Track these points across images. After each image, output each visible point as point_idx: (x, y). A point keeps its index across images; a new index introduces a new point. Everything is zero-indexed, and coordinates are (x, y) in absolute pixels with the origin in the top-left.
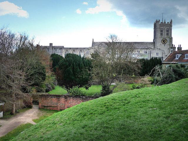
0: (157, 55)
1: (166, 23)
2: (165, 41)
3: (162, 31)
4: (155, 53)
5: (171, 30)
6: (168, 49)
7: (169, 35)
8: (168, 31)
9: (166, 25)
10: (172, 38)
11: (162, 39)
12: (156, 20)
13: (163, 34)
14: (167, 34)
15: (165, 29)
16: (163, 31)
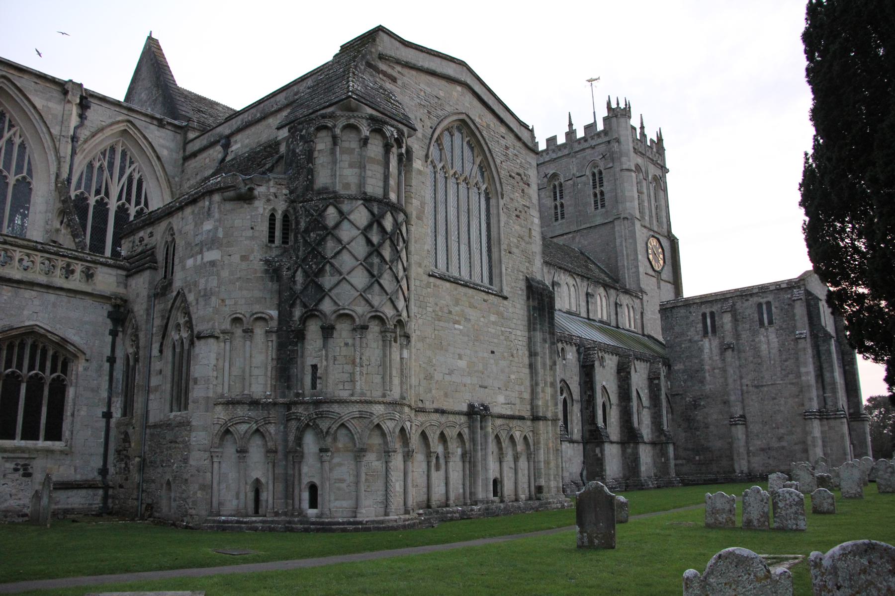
5: (665, 190)
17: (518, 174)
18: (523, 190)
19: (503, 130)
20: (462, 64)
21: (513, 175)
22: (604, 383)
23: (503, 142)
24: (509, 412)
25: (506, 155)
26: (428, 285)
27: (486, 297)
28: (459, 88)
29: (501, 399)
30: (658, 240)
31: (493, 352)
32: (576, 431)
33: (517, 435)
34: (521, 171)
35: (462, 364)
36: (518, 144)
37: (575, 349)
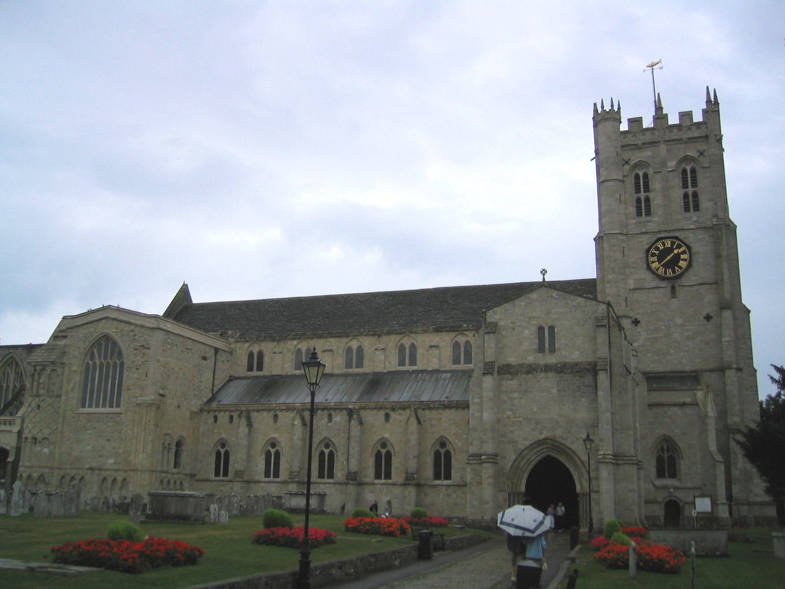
0: (541, 349)
1: (673, 120)
2: (677, 258)
3: (642, 184)
4: (529, 333)
6: (708, 318)
7: (705, 203)
8: (689, 178)
9: (675, 135)
10: (730, 229)
11: (646, 241)
12: (596, 110)
13: (657, 200)
14: (691, 203)
15: (664, 164)
16: (656, 184)
17: (141, 346)
18: (144, 354)
19: (132, 327)
20: (109, 308)
21: (137, 348)
22: (386, 436)
23: (132, 334)
24: (116, 467)
25: (134, 339)
26: (74, 417)
27: (107, 415)
28: (104, 321)
29: (111, 461)
30: (676, 238)
31: (109, 440)
32: (340, 475)
33: (120, 479)
34: (144, 343)
35: (89, 447)
36: (144, 329)
37: (345, 412)
